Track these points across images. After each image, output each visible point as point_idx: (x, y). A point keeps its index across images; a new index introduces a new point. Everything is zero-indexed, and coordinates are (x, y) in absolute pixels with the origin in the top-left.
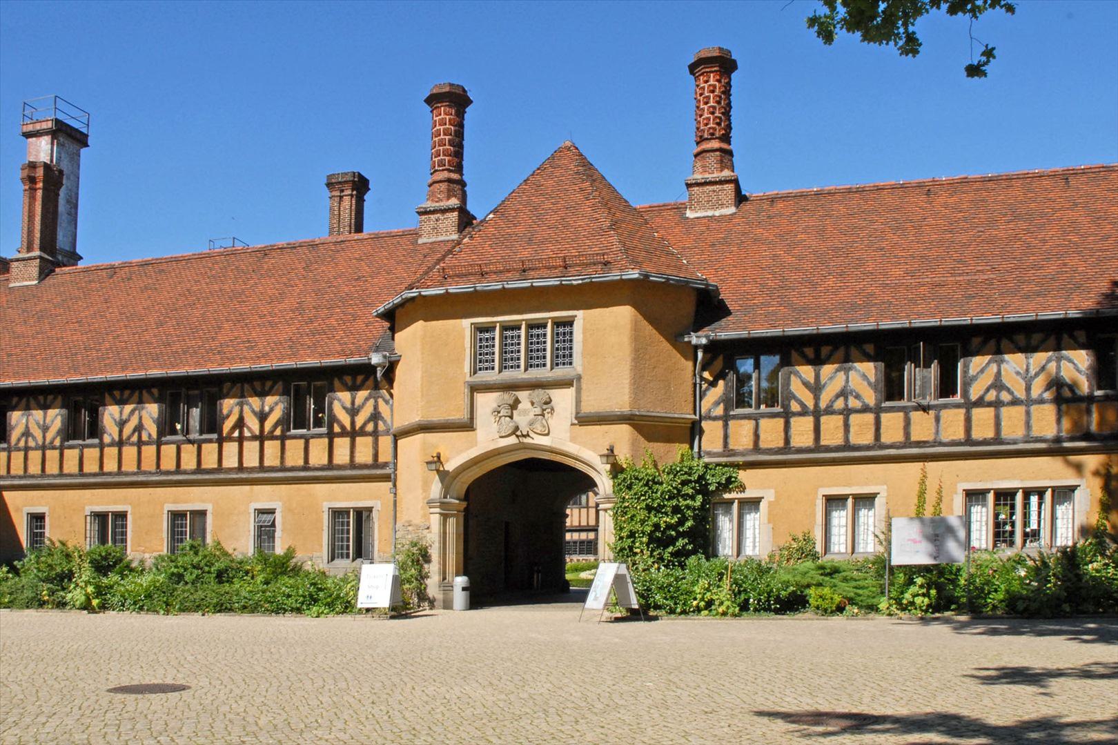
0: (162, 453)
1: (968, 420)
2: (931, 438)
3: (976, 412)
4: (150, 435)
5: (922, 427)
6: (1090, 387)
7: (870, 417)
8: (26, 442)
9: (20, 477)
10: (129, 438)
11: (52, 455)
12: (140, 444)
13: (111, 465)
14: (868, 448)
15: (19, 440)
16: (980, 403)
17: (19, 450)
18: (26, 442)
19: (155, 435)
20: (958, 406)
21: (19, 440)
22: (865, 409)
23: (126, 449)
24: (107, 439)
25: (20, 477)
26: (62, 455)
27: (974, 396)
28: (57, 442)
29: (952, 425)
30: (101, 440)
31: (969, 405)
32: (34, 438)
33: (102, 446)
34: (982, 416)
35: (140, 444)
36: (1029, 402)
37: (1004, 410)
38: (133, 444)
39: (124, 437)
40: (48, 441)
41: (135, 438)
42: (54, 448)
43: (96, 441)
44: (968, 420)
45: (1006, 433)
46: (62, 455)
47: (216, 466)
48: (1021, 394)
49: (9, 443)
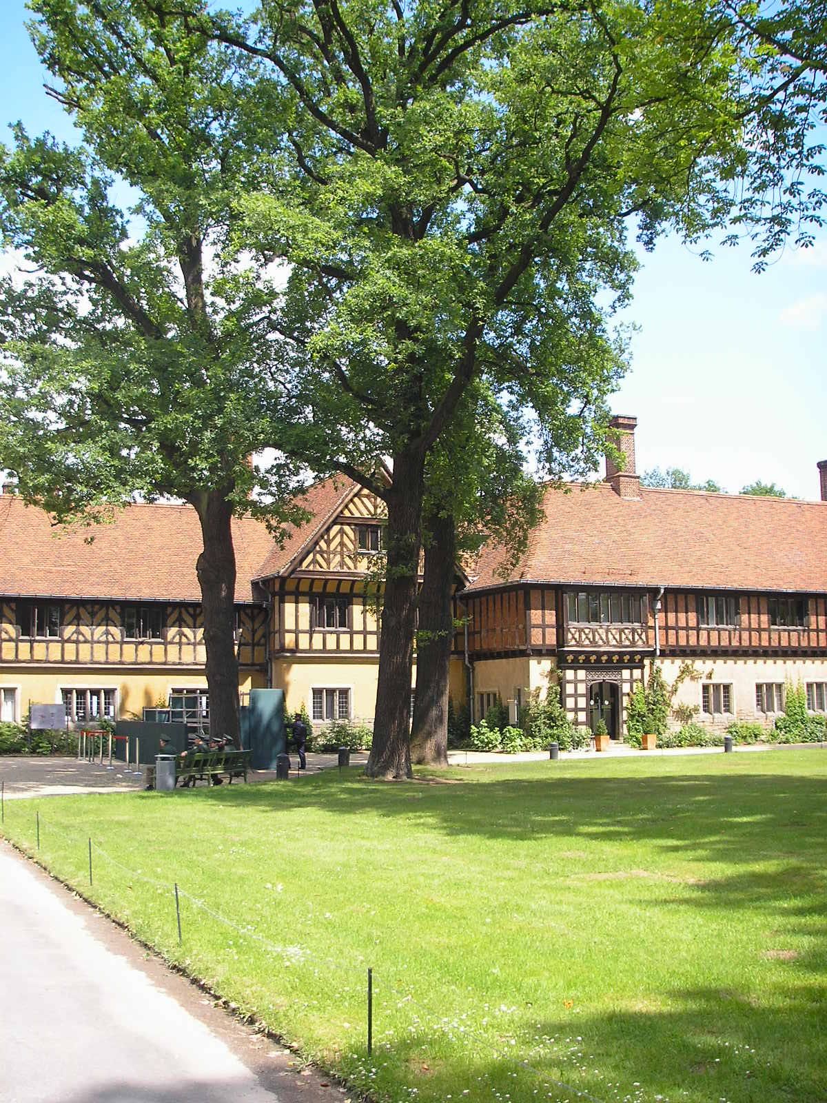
1: (63, 650)
2: (44, 658)
3: (66, 645)
5: (40, 651)
6: (122, 636)
7: (13, 644)
14: (11, 662)
16: (69, 641)
20: (58, 641)
22: (11, 640)
27: (66, 638)
29: (55, 652)
31: (63, 642)
34: (70, 647)
36: (93, 642)
37: (110, 645)
44: (63, 650)
45: (81, 658)
48: (89, 638)
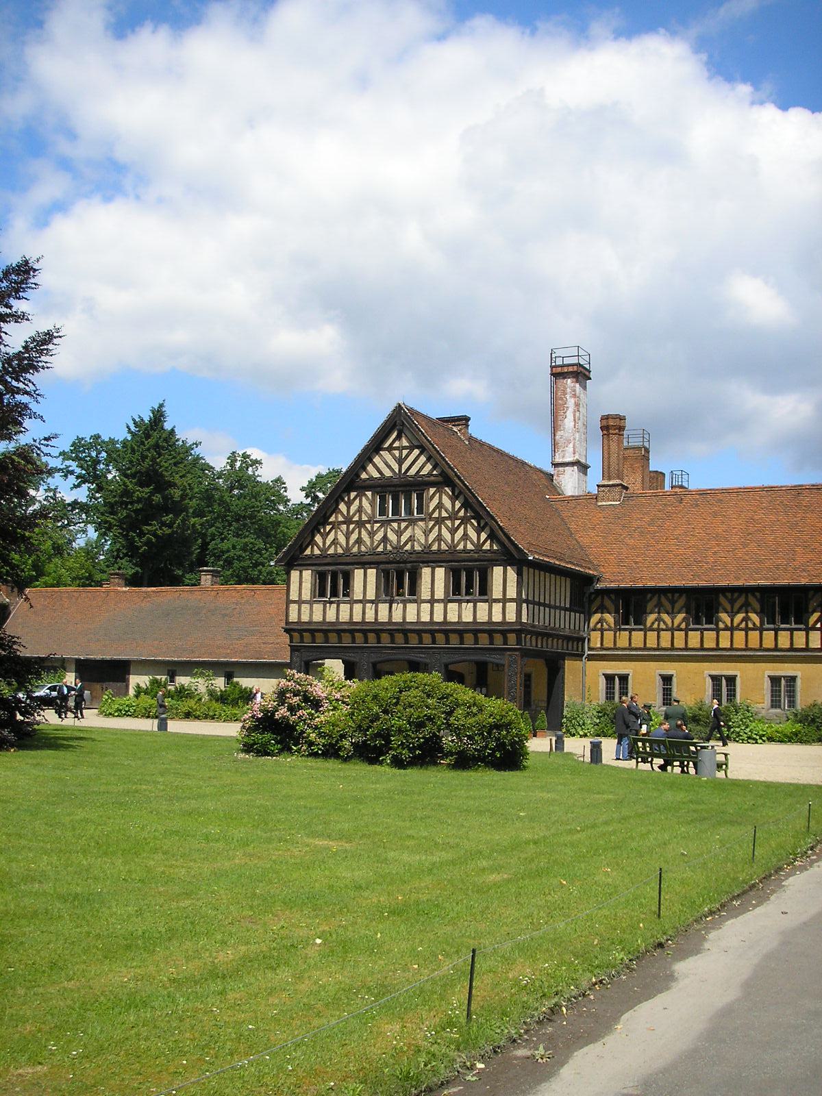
0: (764, 636)
4: (754, 624)
8: (659, 625)
9: (654, 649)
10: (739, 625)
11: (679, 635)
12: (747, 630)
13: (724, 643)
15: (653, 623)
17: (653, 630)
18: (659, 625)
19: (758, 624)
21: (653, 623)
23: (736, 633)
24: (721, 625)
25: (654, 649)
26: (686, 635)
28: (683, 626)
30: (717, 625)
32: (664, 622)
33: (718, 630)
35: (747, 630)
38: (742, 630)
39: (735, 625)
40: (676, 624)
41: (743, 625)
42: (681, 630)
43: (713, 626)
46: (686, 635)
47: (804, 647)
49: (645, 625)
